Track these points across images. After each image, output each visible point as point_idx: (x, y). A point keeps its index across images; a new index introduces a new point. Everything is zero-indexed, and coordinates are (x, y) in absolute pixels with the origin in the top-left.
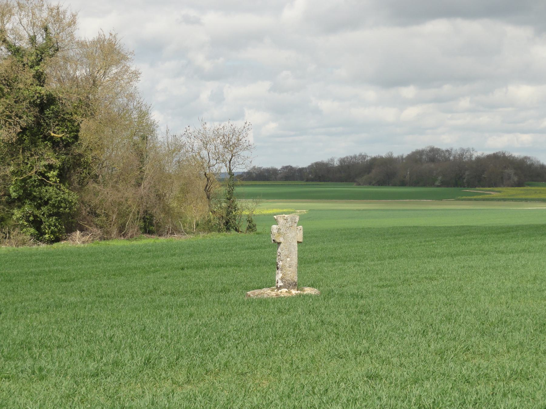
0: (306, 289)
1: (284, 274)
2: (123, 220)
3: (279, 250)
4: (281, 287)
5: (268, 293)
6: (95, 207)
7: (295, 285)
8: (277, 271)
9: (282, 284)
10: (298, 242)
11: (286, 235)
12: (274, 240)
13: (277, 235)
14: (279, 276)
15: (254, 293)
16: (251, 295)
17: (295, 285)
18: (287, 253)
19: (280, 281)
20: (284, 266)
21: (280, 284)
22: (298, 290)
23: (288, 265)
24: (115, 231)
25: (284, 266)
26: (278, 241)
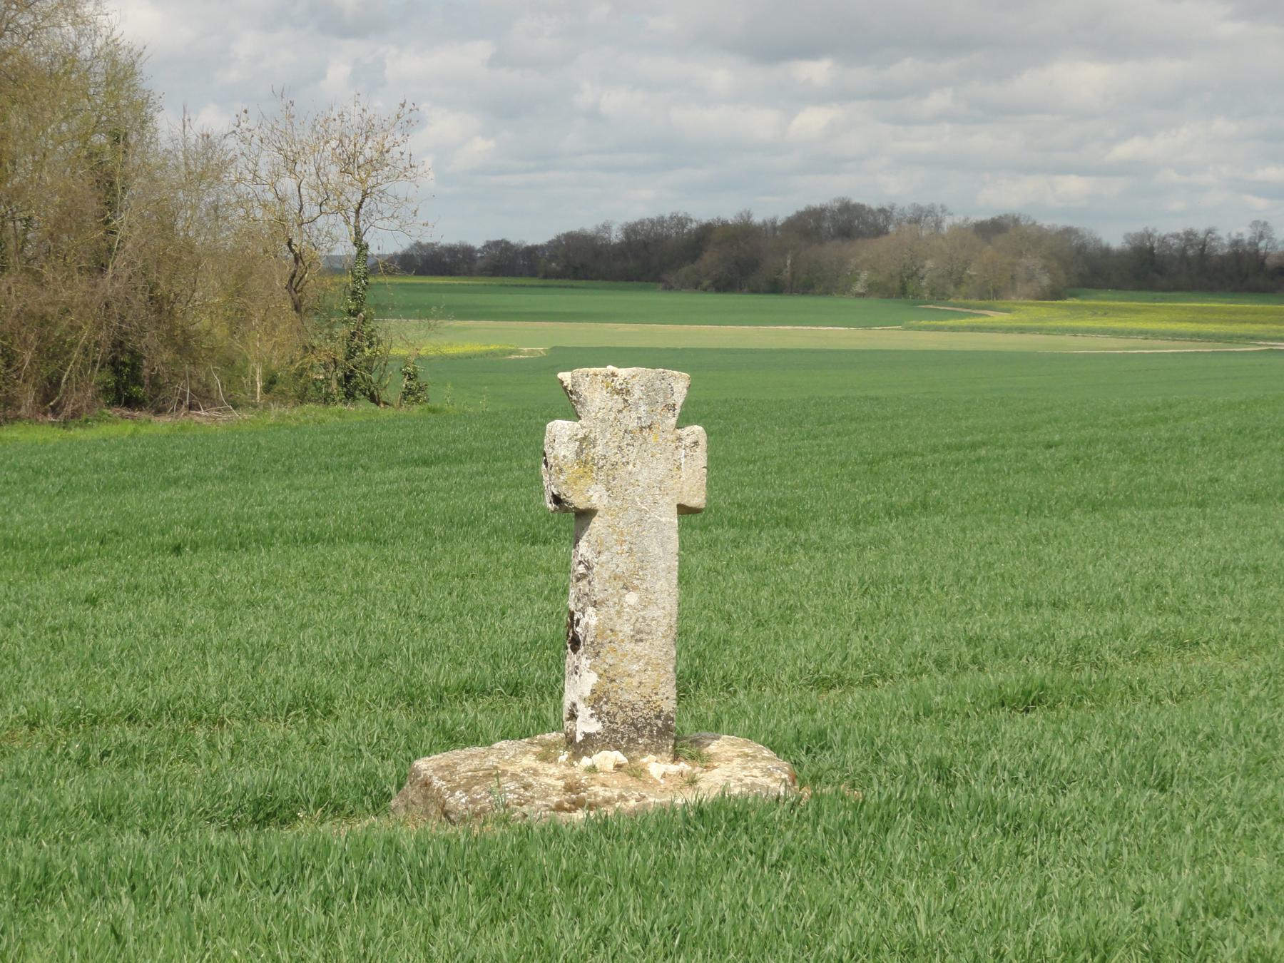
0: (713, 748)
1: (608, 677)
2: (53, 367)
3: (583, 547)
4: (588, 745)
5: (523, 775)
7: (665, 731)
8: (571, 659)
9: (594, 727)
10: (683, 510)
11: (622, 472)
12: (557, 499)
13: (573, 470)
14: (581, 683)
15: (451, 768)
16: (437, 783)
17: (665, 731)
18: (624, 565)
19: (584, 711)
21: (587, 724)
22: (676, 759)
23: (628, 629)
24: (28, 397)
26: (579, 502)
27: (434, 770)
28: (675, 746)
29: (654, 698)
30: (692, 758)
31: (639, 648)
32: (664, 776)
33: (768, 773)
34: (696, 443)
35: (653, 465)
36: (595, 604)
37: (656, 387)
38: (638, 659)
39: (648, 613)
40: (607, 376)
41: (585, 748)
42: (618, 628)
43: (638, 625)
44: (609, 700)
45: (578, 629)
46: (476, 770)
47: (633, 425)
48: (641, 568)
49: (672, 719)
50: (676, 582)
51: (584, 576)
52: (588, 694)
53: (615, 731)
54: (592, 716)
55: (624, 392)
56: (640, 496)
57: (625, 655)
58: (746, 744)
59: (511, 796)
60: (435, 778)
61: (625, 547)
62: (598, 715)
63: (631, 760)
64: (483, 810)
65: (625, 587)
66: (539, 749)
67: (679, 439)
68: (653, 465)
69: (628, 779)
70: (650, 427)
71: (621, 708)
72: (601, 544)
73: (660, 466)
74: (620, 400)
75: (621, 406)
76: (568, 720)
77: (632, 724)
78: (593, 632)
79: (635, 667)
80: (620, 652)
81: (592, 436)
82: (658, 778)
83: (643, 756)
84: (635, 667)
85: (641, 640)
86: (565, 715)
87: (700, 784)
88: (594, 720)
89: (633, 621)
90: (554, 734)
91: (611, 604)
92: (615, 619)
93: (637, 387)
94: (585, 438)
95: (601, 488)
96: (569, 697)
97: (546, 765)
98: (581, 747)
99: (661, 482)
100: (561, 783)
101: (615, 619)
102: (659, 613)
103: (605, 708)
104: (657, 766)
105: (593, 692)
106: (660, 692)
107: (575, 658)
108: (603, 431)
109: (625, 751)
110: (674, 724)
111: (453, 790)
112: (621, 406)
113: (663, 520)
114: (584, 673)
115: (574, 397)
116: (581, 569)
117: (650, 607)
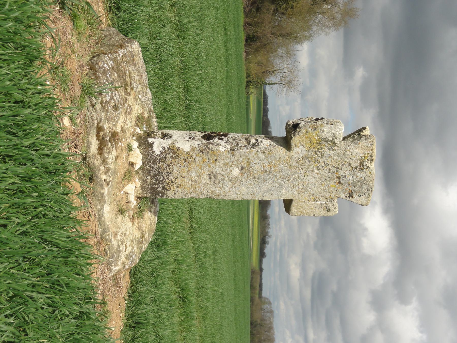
1: (188, 158)
3: (266, 142)
4: (146, 146)
6: (261, 10)
7: (155, 192)
8: (199, 135)
9: (157, 150)
11: (314, 166)
14: (183, 141)
15: (132, 61)
16: (121, 52)
17: (155, 192)
18: (257, 167)
19: (167, 143)
20: (216, 157)
21: (158, 145)
22: (139, 198)
23: (217, 170)
24: (248, 20)
25: (216, 157)
26: (296, 140)
27: (131, 52)
28: (146, 198)
29: (175, 186)
31: (205, 176)
32: (126, 193)
33: (129, 257)
34: (329, 210)
35: (317, 185)
36: (232, 150)
37: (364, 186)
38: (199, 176)
39: (227, 182)
40: (371, 156)
41: (144, 144)
42: (217, 164)
43: (220, 176)
44: (173, 158)
45: (216, 139)
46: (130, 77)
47: (341, 173)
48: (254, 178)
49: (162, 196)
50: (246, 198)
51: (249, 142)
52: (177, 145)
53: (155, 162)
54: (164, 148)
55: (362, 167)
56: (298, 177)
57: (201, 168)
59: (108, 98)
60: (125, 51)
61: (267, 168)
62: (164, 152)
63: (137, 172)
64: (98, 78)
65: (242, 168)
66: (146, 116)
67: (332, 200)
68: (317, 185)
69: (123, 172)
70: (340, 183)
71: (169, 166)
73: (316, 189)
74: (356, 165)
75: (353, 165)
76: (162, 133)
77: (159, 172)
78: (215, 148)
79: (194, 174)
80: (203, 165)
81: (336, 148)
82: (124, 190)
83: (139, 179)
84: (194, 174)
85: (210, 178)
86: (165, 131)
87: (120, 217)
89: (222, 173)
90: (156, 124)
91: (233, 160)
92: (223, 162)
93: (364, 174)
94: (334, 143)
95: (304, 153)
96: (176, 134)
97: (134, 119)
98: (145, 142)
99: (306, 190)
100: (118, 129)
101: (223, 162)
102: (227, 189)
103: (168, 156)
104: (133, 189)
105: (178, 149)
106: (179, 189)
107: (199, 137)
108: (338, 154)
109: (142, 168)
110: (159, 197)
111: (115, 60)
112: (353, 165)
113: (283, 191)
114: (190, 143)
115: (356, 137)
116: (253, 141)
117: (230, 183)
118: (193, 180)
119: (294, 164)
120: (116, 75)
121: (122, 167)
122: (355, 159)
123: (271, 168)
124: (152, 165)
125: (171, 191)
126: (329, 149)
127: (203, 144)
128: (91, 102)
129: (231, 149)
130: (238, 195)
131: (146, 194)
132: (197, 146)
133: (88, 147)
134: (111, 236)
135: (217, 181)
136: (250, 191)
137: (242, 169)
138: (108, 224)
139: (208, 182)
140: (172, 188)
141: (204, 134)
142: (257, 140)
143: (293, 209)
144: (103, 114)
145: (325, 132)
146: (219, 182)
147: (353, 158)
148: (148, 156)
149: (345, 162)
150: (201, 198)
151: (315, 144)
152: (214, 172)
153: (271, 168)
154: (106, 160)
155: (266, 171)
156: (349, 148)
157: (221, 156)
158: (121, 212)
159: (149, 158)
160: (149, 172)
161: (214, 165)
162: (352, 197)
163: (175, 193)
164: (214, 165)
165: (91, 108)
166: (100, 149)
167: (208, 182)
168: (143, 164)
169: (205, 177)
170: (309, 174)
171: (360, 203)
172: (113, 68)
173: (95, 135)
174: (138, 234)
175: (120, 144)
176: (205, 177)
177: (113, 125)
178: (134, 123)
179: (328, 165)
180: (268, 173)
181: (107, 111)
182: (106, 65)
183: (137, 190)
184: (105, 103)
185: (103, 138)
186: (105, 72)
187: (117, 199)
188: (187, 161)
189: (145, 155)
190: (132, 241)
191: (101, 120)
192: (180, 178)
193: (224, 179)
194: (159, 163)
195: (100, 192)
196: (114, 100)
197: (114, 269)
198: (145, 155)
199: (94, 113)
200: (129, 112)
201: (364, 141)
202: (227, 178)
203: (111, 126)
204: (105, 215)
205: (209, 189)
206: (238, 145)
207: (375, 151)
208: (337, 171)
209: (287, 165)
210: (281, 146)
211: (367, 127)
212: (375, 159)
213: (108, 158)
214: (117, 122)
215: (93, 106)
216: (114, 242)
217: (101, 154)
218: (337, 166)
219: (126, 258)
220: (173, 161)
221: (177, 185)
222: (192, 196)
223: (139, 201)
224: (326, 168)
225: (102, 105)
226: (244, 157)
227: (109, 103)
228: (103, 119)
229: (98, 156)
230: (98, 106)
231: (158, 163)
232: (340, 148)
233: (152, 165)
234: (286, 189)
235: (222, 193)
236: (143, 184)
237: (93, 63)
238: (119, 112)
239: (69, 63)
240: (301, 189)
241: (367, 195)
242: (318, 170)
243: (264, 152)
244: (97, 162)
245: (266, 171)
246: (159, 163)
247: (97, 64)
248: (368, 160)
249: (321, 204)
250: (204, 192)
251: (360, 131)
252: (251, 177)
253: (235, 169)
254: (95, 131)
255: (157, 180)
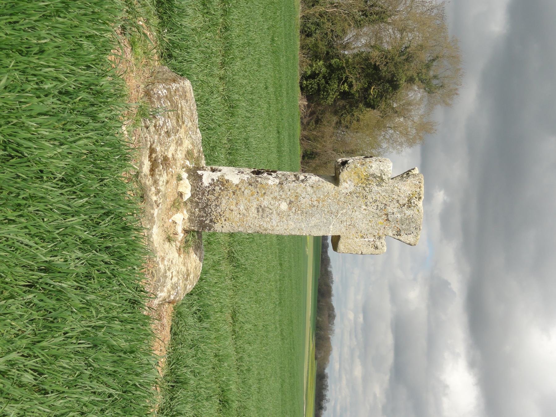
1: (237, 191)
2: (312, 139)
4: (195, 176)
6: (321, 122)
7: (202, 225)
11: (361, 202)
12: (344, 163)
14: (232, 175)
16: (174, 86)
17: (202, 225)
18: (305, 202)
19: (216, 176)
20: (264, 191)
21: (207, 177)
22: (186, 231)
23: (265, 203)
24: (305, 133)
25: (264, 191)
26: (344, 175)
27: (183, 88)
28: (194, 231)
29: (223, 219)
30: (187, 242)
31: (253, 210)
32: (174, 222)
33: (174, 287)
34: (377, 248)
35: (365, 221)
36: (281, 183)
37: (412, 224)
38: (247, 209)
39: (274, 216)
40: (419, 194)
42: (266, 197)
43: (268, 210)
44: (222, 191)
45: (265, 174)
46: (182, 111)
47: (389, 209)
48: (302, 212)
49: (210, 230)
50: (293, 233)
51: (298, 179)
52: (226, 178)
53: (203, 193)
54: (213, 180)
55: (409, 204)
56: (346, 212)
57: (249, 201)
58: (196, 275)
59: (161, 123)
61: (315, 203)
62: (213, 184)
63: (185, 203)
64: (152, 102)
67: (380, 238)
69: (172, 199)
70: (388, 220)
71: (217, 198)
72: (317, 188)
73: (363, 226)
74: (404, 202)
75: (401, 202)
76: (211, 168)
77: (207, 205)
78: (264, 182)
79: (242, 208)
80: (251, 198)
81: (384, 184)
82: (172, 218)
83: (187, 211)
84: (242, 208)
85: (258, 212)
86: (214, 167)
87: (167, 244)
88: (210, 181)
89: (270, 207)
92: (272, 196)
93: (412, 212)
94: (382, 180)
95: (352, 188)
96: (225, 170)
97: (184, 153)
100: (170, 156)
101: (272, 196)
103: (217, 188)
104: (181, 219)
105: (227, 181)
106: (226, 223)
108: (386, 191)
109: (190, 200)
110: (207, 231)
111: (168, 90)
112: (401, 202)
113: (331, 227)
114: (239, 176)
115: (405, 175)
116: (302, 177)
118: (241, 213)
119: (342, 199)
120: (169, 104)
121: (170, 192)
122: (403, 196)
123: (319, 203)
124: (200, 197)
125: (218, 224)
126: (377, 185)
127: (252, 177)
128: (145, 123)
129: (280, 183)
130: (285, 229)
131: (194, 226)
132: (246, 179)
133: (141, 167)
134: (158, 259)
135: (265, 215)
136: (298, 226)
137: (290, 203)
138: (156, 246)
139: (256, 216)
140: (220, 221)
141: (253, 170)
142: (306, 177)
143: (341, 246)
144: (156, 137)
145: (373, 168)
146: (267, 216)
147: (401, 195)
148: (197, 187)
149: (393, 199)
150: (249, 232)
151: (363, 180)
152: (262, 206)
153: (319, 203)
154: (158, 182)
155: (314, 206)
156: (397, 185)
157: (269, 189)
158: (169, 239)
159: (198, 189)
160: (197, 204)
161: (262, 199)
162: (400, 235)
163: (223, 227)
164: (262, 199)
165: (145, 130)
166: (152, 170)
167: (256, 216)
168: (192, 195)
169: (253, 210)
170: (357, 210)
171: (408, 242)
172: (167, 96)
173: (148, 156)
174: (184, 269)
175: (171, 169)
176: (253, 210)
177: (165, 150)
178: (184, 156)
179: (376, 201)
180: (316, 207)
181: (160, 134)
182: (160, 92)
183: (185, 223)
184: (159, 127)
185: (155, 160)
186: (159, 98)
187: (165, 226)
188: (236, 194)
189: (194, 187)
190: (178, 272)
191: (154, 142)
192: (228, 211)
193: (272, 213)
194: (208, 195)
195: (150, 212)
196: (167, 126)
197: (160, 295)
198: (194, 187)
199: (147, 135)
200: (179, 143)
201: (412, 179)
202: (275, 212)
203: (163, 150)
204: (153, 236)
205: (257, 223)
206: (287, 179)
207: (423, 189)
208: (385, 208)
209: (335, 200)
210: (329, 182)
211: (416, 168)
212: (423, 197)
213: (159, 180)
214: (169, 147)
215: (147, 128)
216: (161, 266)
217: (152, 175)
218: (385, 202)
219: (172, 287)
220: (222, 193)
221: (224, 218)
222: (240, 230)
223: (185, 236)
224: (374, 204)
225: (155, 128)
226: (293, 191)
227: (162, 127)
228: (156, 141)
229: (150, 177)
230: (152, 129)
231: (206, 195)
232: (388, 185)
233: (200, 197)
234: (334, 225)
235: (269, 228)
236: (191, 216)
237: (148, 90)
238: (171, 139)
239: (128, 81)
240: (349, 225)
241: (415, 234)
242: (366, 206)
243: (312, 187)
244: (149, 182)
245: (314, 206)
246: (208, 195)
247: (152, 90)
248: (416, 198)
249: (369, 241)
250: (252, 226)
251: (410, 171)
252: (299, 212)
253: (283, 203)
254: (148, 152)
255: (205, 213)
